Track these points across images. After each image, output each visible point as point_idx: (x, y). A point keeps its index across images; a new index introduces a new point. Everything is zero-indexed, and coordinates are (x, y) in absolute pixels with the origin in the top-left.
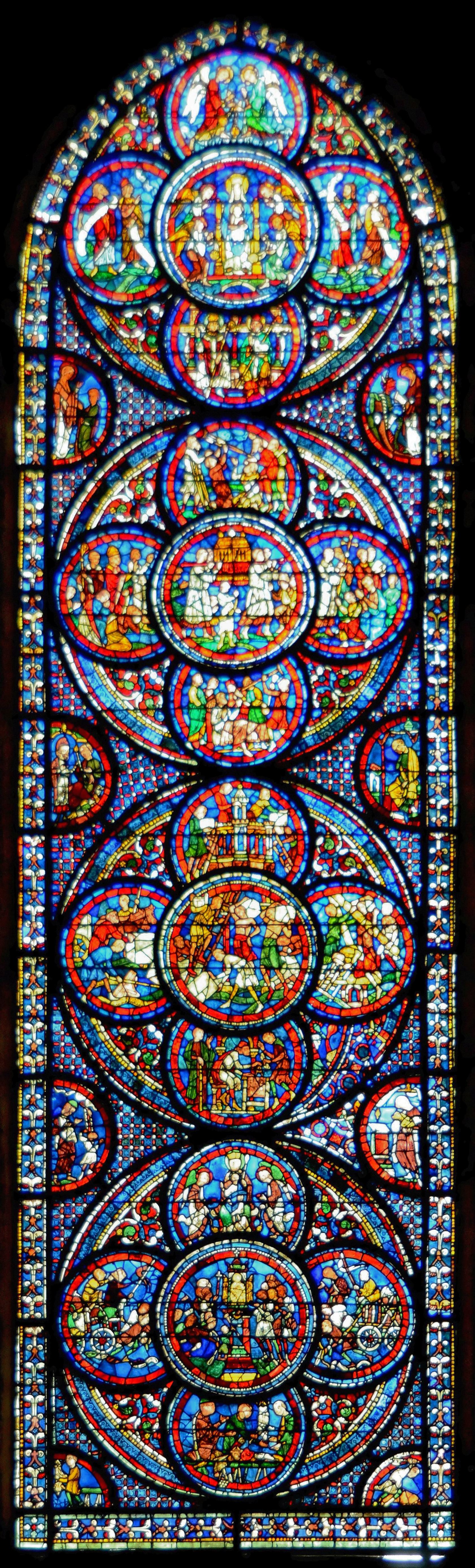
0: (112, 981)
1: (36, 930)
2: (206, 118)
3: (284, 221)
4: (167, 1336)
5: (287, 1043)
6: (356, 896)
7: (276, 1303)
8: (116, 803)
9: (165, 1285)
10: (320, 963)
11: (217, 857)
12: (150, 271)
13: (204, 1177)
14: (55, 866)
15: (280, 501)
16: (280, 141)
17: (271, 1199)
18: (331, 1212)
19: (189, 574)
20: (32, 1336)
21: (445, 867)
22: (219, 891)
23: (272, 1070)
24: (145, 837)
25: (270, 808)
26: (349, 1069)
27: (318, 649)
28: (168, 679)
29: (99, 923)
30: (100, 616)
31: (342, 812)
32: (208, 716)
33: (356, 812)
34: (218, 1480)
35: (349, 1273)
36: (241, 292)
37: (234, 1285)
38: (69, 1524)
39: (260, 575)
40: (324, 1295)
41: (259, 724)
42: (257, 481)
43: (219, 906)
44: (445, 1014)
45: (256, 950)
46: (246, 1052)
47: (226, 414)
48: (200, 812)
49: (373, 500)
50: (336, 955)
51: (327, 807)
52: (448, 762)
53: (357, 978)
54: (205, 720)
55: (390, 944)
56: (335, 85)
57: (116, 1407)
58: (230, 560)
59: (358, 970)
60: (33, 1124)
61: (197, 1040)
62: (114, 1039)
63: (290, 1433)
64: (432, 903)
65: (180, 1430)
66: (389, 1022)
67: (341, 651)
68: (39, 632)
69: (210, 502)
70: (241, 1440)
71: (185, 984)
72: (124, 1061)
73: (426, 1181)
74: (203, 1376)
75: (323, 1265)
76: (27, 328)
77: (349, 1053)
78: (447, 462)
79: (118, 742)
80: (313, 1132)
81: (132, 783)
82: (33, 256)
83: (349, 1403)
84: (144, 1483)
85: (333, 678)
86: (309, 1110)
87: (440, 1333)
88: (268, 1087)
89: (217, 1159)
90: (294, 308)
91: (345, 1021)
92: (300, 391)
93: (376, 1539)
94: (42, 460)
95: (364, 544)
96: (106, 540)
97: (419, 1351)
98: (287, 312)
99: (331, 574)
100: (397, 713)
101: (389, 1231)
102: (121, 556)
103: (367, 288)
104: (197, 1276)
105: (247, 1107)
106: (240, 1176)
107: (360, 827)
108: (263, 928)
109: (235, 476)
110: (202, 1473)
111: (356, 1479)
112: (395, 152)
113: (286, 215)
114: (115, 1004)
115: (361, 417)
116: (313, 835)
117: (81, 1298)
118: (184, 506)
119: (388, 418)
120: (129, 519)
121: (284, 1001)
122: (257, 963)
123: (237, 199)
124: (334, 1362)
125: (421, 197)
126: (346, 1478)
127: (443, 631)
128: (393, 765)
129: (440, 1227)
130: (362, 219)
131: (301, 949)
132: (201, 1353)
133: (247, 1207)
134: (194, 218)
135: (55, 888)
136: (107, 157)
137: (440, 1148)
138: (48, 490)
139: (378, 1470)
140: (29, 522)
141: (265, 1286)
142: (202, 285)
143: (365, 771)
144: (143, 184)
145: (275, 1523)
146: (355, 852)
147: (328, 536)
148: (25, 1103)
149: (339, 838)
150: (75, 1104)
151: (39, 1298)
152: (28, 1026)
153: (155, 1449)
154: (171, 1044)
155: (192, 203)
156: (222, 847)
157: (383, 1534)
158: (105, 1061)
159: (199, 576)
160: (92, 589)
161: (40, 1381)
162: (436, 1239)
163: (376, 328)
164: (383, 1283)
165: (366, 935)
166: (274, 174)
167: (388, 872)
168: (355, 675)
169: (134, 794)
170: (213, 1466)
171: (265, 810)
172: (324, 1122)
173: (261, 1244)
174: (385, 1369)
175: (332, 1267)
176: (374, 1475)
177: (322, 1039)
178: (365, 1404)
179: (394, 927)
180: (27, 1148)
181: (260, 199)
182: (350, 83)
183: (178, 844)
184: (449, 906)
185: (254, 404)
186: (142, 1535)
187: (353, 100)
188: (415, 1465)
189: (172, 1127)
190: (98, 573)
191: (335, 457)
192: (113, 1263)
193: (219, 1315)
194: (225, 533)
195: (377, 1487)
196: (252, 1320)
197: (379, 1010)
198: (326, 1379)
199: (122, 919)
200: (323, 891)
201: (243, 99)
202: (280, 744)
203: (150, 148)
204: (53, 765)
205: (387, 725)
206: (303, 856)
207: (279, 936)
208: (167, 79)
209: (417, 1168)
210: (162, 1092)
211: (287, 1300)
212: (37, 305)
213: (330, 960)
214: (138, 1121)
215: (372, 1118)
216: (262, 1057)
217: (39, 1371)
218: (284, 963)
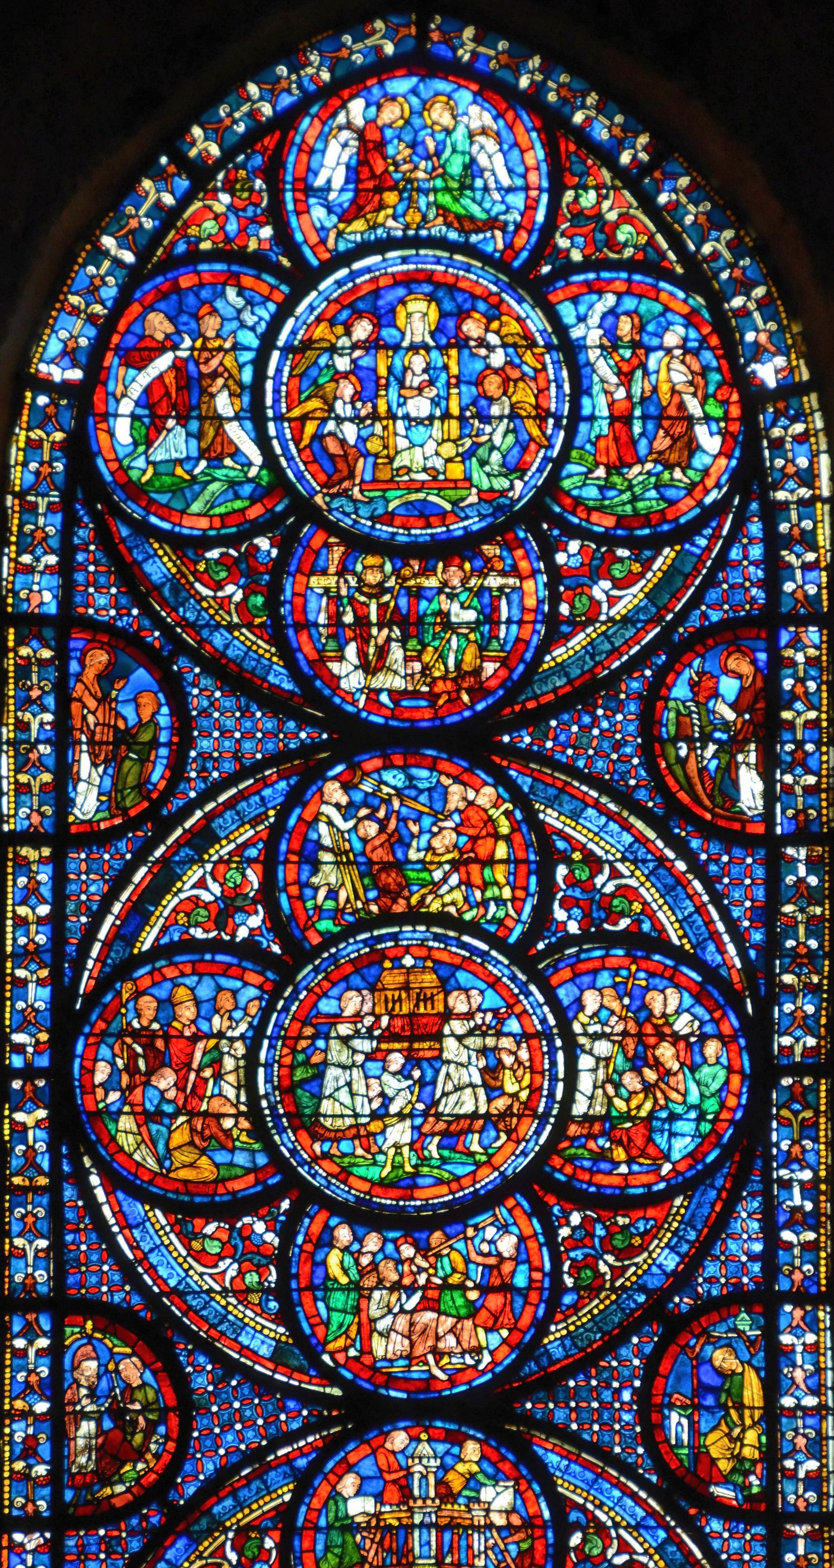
2: (357, 191)
3: (506, 381)
8: (188, 1467)
12: (253, 472)
15: (500, 901)
16: (498, 234)
19: (327, 1038)
25: (481, 1477)
27: (571, 1177)
28: (287, 1234)
30: (157, 1116)
31: (618, 1485)
32: (364, 1304)
33: (643, 1483)
36: (425, 514)
39: (460, 1038)
42: (455, 865)
47: (399, 739)
48: (348, 1484)
49: (675, 898)
51: (589, 1475)
52: (816, 1392)
54: (357, 1311)
56: (601, 133)
58: (405, 1010)
67: (616, 1181)
68: (41, 1146)
69: (367, 902)
76: (20, 579)
78: (815, 828)
79: (190, 1353)
81: (217, 1430)
82: (33, 445)
85: (600, 1231)
90: (522, 543)
92: (536, 697)
94: (46, 822)
95: (657, 981)
96: (170, 973)
98: (511, 550)
99: (595, 1037)
100: (721, 1297)
102: (198, 1003)
103: (663, 505)
107: (651, 1513)
109: (413, 855)
112: (715, 255)
113: (508, 370)
115: (651, 743)
116: (564, 1529)
118: (318, 909)
119: (703, 748)
120: (212, 935)
123: (418, 339)
125: (763, 338)
127: (808, 1144)
128: (715, 1397)
130: (653, 378)
134: (338, 376)
136: (171, 263)
138: (60, 879)
140: (22, 941)
142: (351, 498)
143: (662, 1406)
144: (239, 311)
147: (590, 965)
149: (613, 1533)
155: (333, 349)
156: (390, 1550)
159: (345, 1040)
160: (142, 1064)
163: (679, 582)
166: (487, 296)
168: (641, 1226)
169: (222, 1452)
181: (461, 343)
182: (629, 131)
183: (306, 1544)
185: (449, 720)
187: (634, 157)
190: (153, 1035)
191: (603, 819)
194: (397, 960)
201: (428, 158)
202: (500, 1356)
203: (253, 245)
204: (69, 1395)
205: (703, 1321)
208: (286, 121)
212: (39, 535)
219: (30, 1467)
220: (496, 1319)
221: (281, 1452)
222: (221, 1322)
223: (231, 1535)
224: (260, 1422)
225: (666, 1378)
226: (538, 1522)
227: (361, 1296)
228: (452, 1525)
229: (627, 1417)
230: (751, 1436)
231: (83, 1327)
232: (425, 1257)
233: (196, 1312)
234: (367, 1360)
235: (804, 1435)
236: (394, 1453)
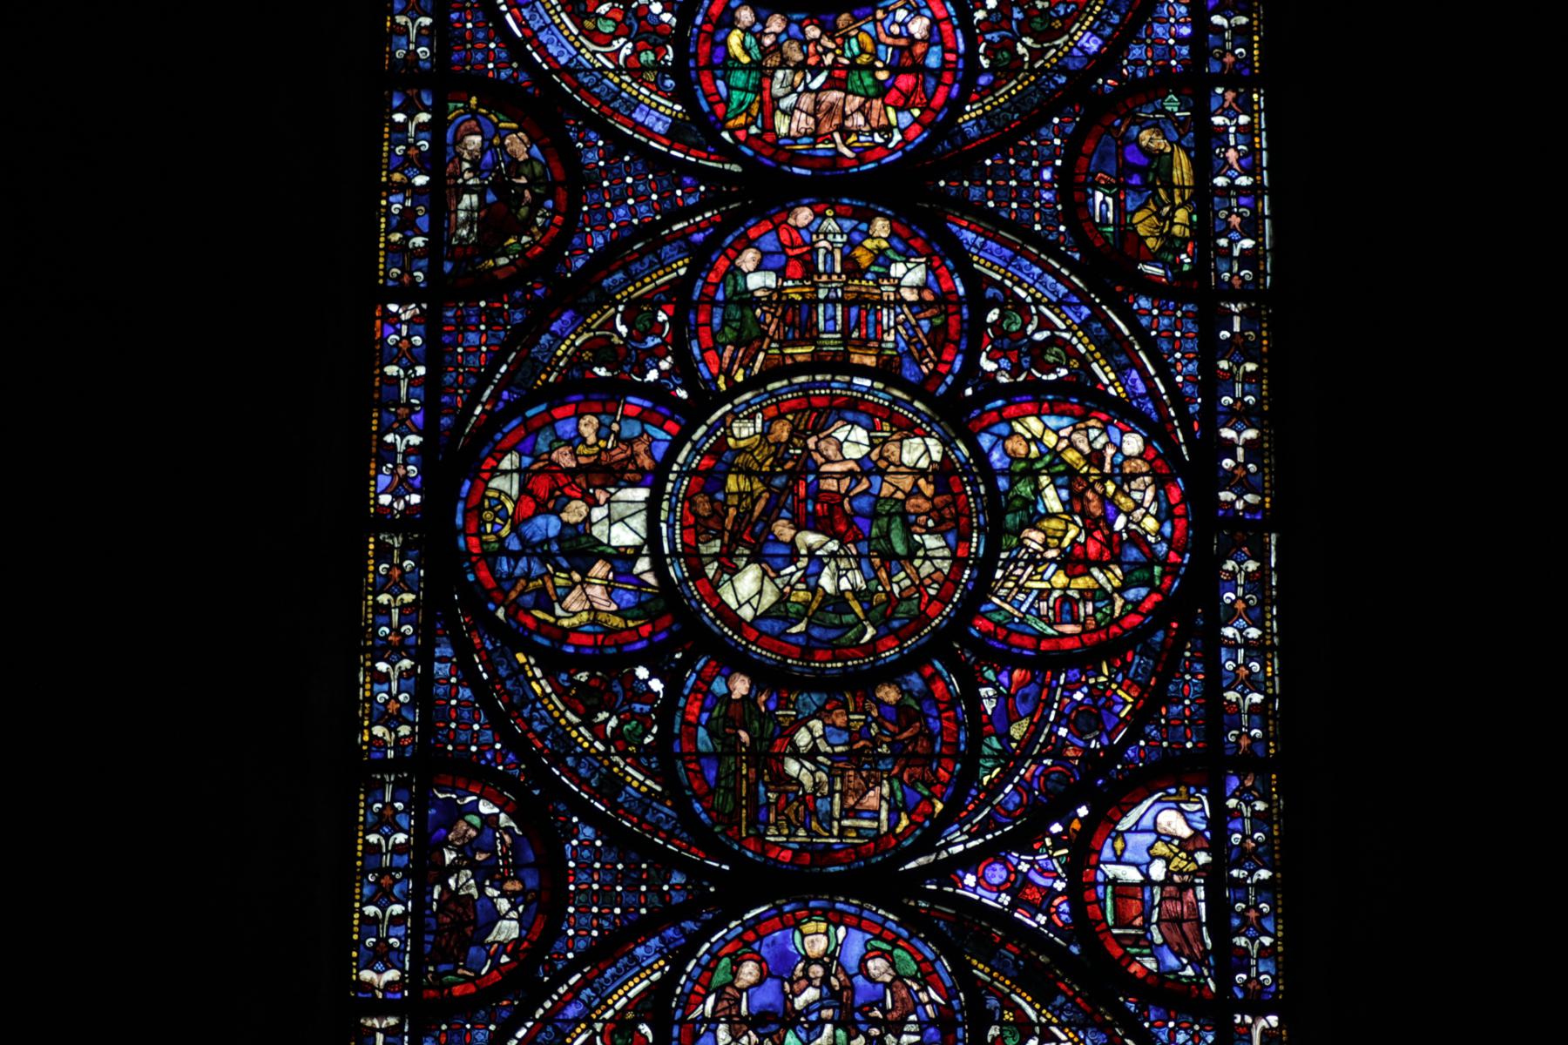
1: (406, 477)
5: (926, 705)
6: (1066, 421)
8: (576, 241)
10: (993, 548)
11: (783, 343)
13: (749, 972)
14: (448, 358)
21: (1251, 367)
24: (633, 306)
25: (890, 253)
29: (536, 467)
31: (1037, 262)
32: (766, 83)
33: (1065, 261)
41: (868, 98)
43: (785, 435)
45: (862, 523)
46: (840, 721)
48: (749, 259)
51: (1007, 252)
53: (1071, 576)
54: (758, 89)
55: (1138, 513)
60: (386, 860)
61: (736, 695)
62: (561, 692)
64: (1227, 433)
71: (715, 585)
73: (1225, 982)
77: (1057, 723)
79: (580, 129)
81: (608, 205)
85: (1017, 14)
88: (886, 790)
91: (1047, 661)
100: (1146, 78)
105: (842, 829)
107: (1073, 289)
108: (876, 480)
114: (565, 623)
121: (921, 619)
122: (864, 547)
131: (956, 519)
133: (840, 1033)
135: (445, 399)
137: (1253, 914)
146: (1067, 336)
149: (1033, 310)
150: (476, 820)
152: (382, 666)
154: (682, 703)
156: (792, 325)
158: (541, 736)
165: (1090, 495)
167: (1134, 374)
169: (613, 226)
171: (881, 258)
172: (1005, 862)
177: (999, 694)
180: (370, 910)
183: (702, 318)
189: (680, 871)
199: (583, 460)
200: (999, 410)
204: (450, 168)
206: (957, 344)
207: (909, 495)
210: (660, 798)
215: (1107, 853)
218: (923, 545)
219: (407, 239)
220: (907, 99)
222: (614, 99)
223: (621, 308)
225: (1090, 158)
226: (953, 298)
227: (763, 75)
228: (860, 300)
229: (1046, 195)
231: (467, 102)
232: (832, 39)
233: (588, 89)
235: (1238, 214)
236: (797, 228)
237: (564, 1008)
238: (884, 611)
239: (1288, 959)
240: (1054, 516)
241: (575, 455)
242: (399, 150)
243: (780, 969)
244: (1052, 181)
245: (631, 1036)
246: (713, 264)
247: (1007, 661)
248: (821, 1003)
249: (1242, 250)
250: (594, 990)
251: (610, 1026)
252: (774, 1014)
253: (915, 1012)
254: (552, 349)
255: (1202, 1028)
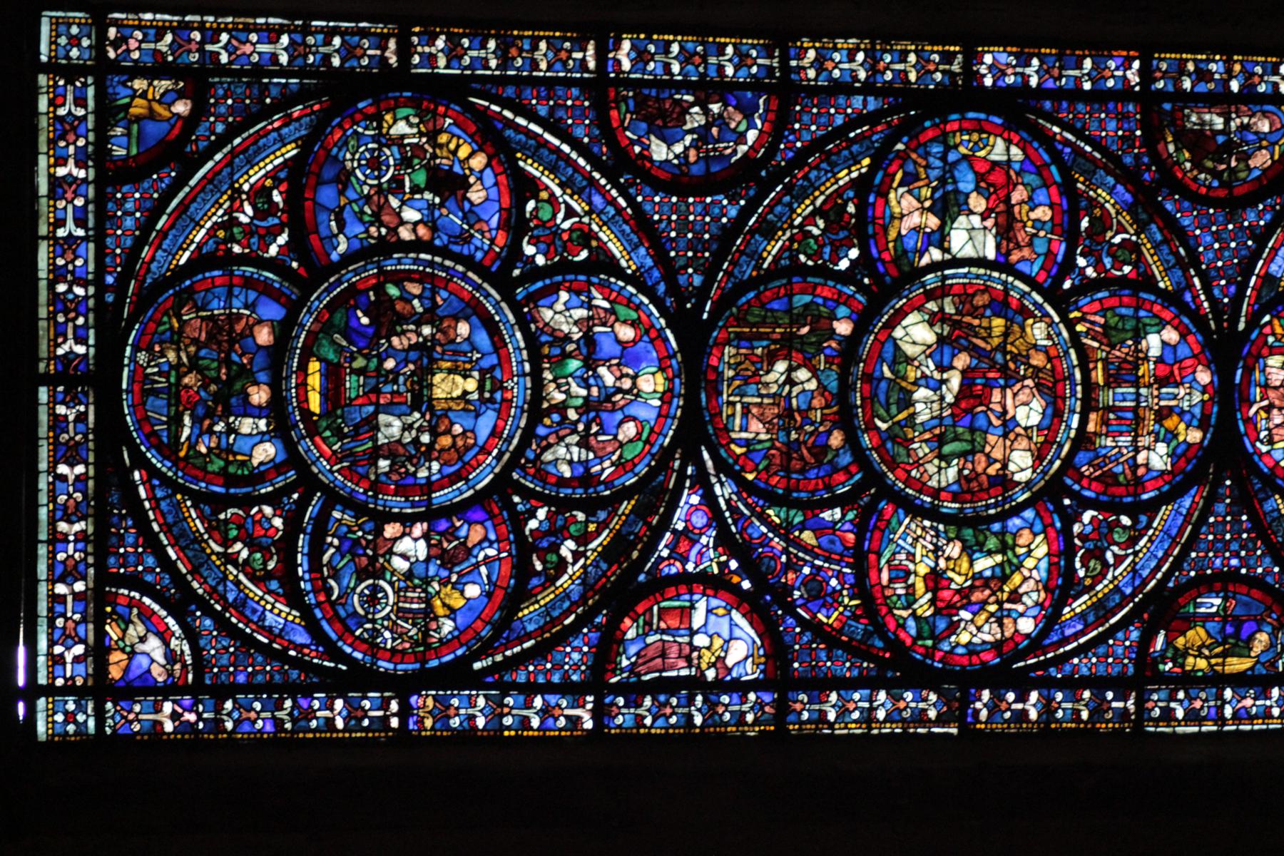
0: (926, 192)
1: (1004, 74)
4: (380, 268)
5: (828, 468)
6: (1044, 575)
7: (430, 447)
8: (1186, 204)
9: (460, 268)
10: (947, 519)
11: (1106, 361)
13: (626, 333)
14: (1096, 106)
17: (592, 441)
18: (572, 537)
20: (384, 48)
21: (1085, 715)
22: (1056, 362)
23: (788, 444)
24: (1134, 248)
25: (1174, 443)
26: (788, 567)
29: (1012, 173)
31: (1167, 554)
33: (1167, 576)
34: (149, 349)
35: (477, 565)
37: (459, 379)
38: (80, 101)
40: (443, 525)
43: (1034, 362)
44: (868, 717)
45: (967, 419)
46: (816, 403)
48: (1171, 335)
50: (958, 545)
51: (1174, 532)
52: (1236, 716)
55: (973, 629)
57: (269, 182)
59: (936, 580)
60: (713, 60)
61: (835, 324)
62: (839, 192)
63: (224, 469)
64: (1034, 696)
65: (230, 287)
66: (859, 628)
70: (213, 387)
71: (920, 308)
72: (805, 209)
73: (619, 689)
74: (316, 327)
75: (488, 524)
77: (813, 566)
79: (1273, 207)
80: (696, 508)
81: (1214, 228)
83: (271, 565)
84: (146, 226)
86: (728, 502)
87: (380, 713)
88: (763, 437)
89: (654, 354)
91: (861, 559)
93: (50, 610)
97: (357, 679)
101: (541, 630)
104: (474, 319)
105: (734, 404)
106: (629, 392)
107: (1145, 582)
108: (1000, 431)
110: (161, 323)
111: (149, 578)
114: (892, 195)
116: (1133, 511)
117: (441, 131)
121: (893, 464)
122: (948, 421)
124: (336, 542)
126: (150, 561)
129: (546, 712)
131: (969, 491)
132: (353, 324)
133: (579, 402)
135: (1065, 105)
139: (163, 613)
141: (457, 429)
143: (1226, 590)
145: (78, 443)
146: (1110, 576)
148: (744, 48)
149: (1130, 551)
150: (742, 127)
151: (442, 62)
152: (860, 56)
153: (200, 246)
154: (831, 283)
156: (1119, 368)
157: (60, 622)
158: (806, 177)
161: (311, 59)
162: (528, 705)
164: (459, 620)
165: (987, 592)
167: (1080, 627)
169: (1198, 232)
170: (172, 342)
171: (1172, 435)
172: (708, 526)
173: (523, 424)
174: (324, 624)
175: (486, 539)
176: (156, 607)
177: (836, 523)
178: (270, 592)
179: (999, 636)
180: (675, 48)
183: (1126, 300)
184: (1029, 721)
186: (61, 223)
188: (170, 674)
189: (704, 282)
192: (496, 184)
193: (413, 355)
195: (135, 611)
196: (404, 408)
197: (877, 612)
198: (309, 529)
199: (1017, 209)
200: (1053, 525)
202: (1266, 459)
204: (1244, 108)
206: (1104, 493)
207: (988, 456)
209: (639, 675)
210: (758, 267)
211: (435, 466)
213: (952, 535)
214: (714, 230)
215: (715, 602)
216: (808, 428)
217: (327, 58)
218: (949, 466)
219: (1189, 75)
221: (1196, 281)
223: (1134, 238)
224: (1220, 264)
225: (1247, 595)
226: (1139, 489)
228: (1138, 420)
230: (1202, 664)
234: (1265, 351)
235: (1202, 707)
236: (1194, 372)
237: (600, 193)
238: (898, 436)
239: (634, 739)
240: (971, 565)
241: (1021, 203)
242: (1258, 70)
243: (627, 355)
244: (1228, 565)
245: (579, 244)
246: (1167, 308)
247: (861, 528)
248: (601, 387)
249: (1174, 710)
250: (613, 217)
251: (586, 230)
252: (594, 352)
253: (596, 457)
254: (1102, 185)
255: (583, 672)
